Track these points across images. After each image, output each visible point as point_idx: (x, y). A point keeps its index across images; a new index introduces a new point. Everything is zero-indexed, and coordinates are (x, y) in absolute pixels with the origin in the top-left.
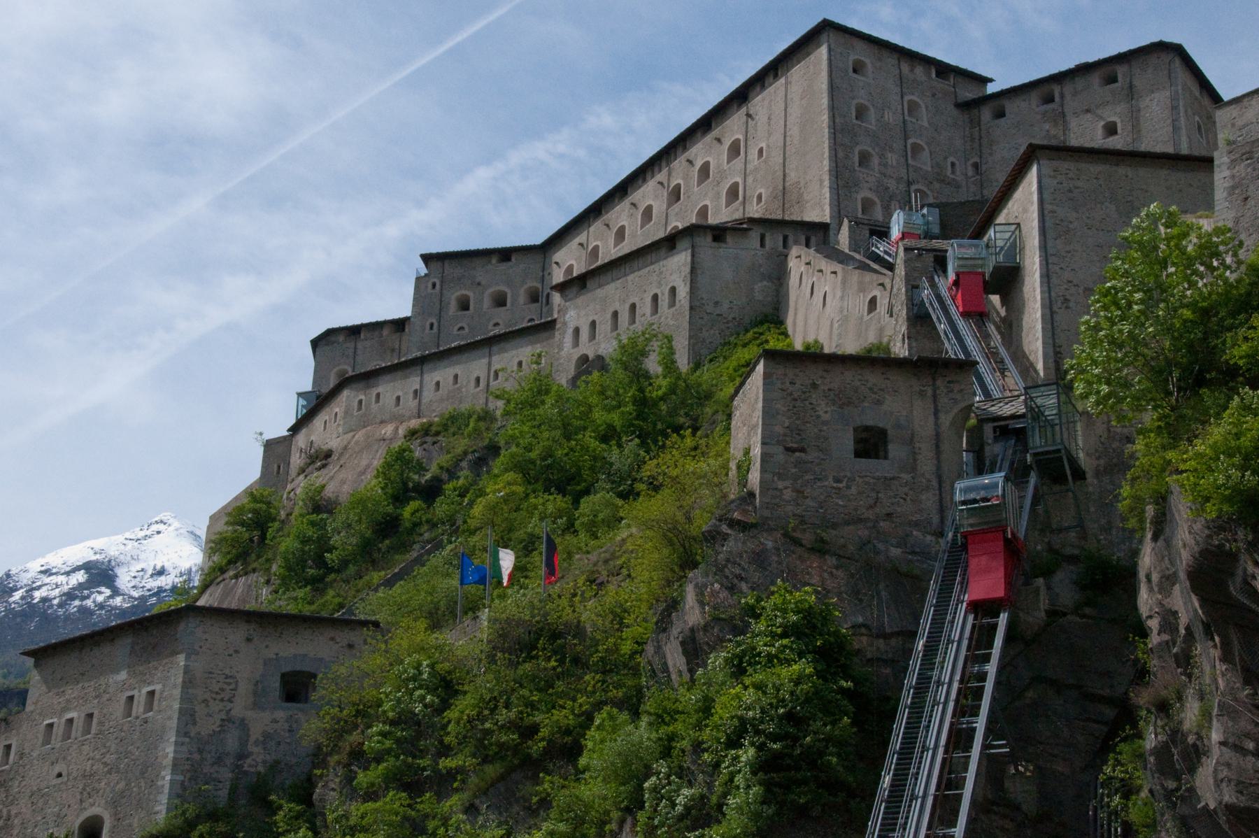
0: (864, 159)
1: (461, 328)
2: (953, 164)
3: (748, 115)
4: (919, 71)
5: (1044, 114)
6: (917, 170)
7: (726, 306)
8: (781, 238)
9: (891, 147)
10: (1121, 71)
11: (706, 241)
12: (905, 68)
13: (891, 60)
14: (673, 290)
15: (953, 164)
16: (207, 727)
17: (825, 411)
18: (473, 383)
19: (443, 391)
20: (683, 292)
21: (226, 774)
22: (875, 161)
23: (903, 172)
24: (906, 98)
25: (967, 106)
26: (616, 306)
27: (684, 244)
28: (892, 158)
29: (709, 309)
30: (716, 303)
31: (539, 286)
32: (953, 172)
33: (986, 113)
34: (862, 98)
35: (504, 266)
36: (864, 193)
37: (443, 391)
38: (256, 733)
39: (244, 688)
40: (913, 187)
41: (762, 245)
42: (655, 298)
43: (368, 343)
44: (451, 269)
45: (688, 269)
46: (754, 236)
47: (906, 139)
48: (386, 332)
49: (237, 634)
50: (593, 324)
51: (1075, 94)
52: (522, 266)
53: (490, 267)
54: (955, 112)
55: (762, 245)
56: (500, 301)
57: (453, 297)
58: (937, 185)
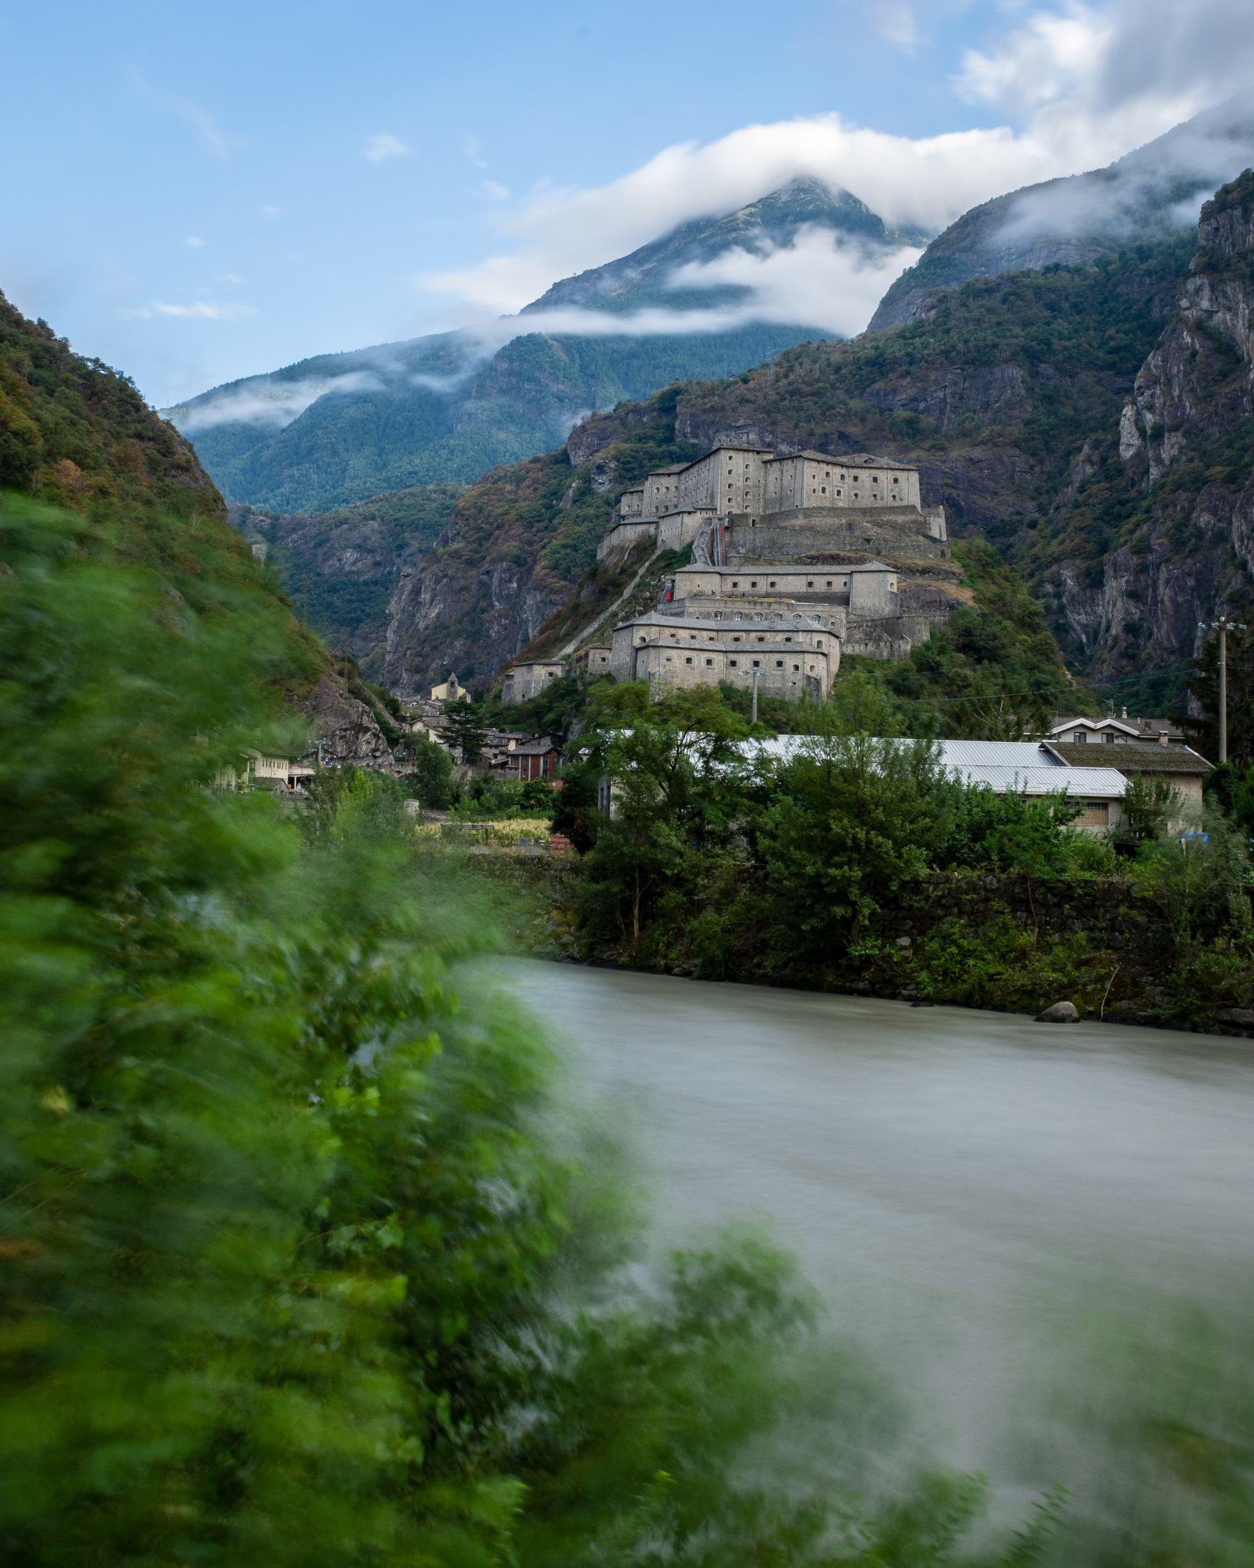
11: (686, 516)
13: (741, 454)
25: (765, 462)
28: (740, 484)
33: (769, 465)
44: (655, 479)
46: (699, 512)
56: (667, 488)
57: (655, 487)
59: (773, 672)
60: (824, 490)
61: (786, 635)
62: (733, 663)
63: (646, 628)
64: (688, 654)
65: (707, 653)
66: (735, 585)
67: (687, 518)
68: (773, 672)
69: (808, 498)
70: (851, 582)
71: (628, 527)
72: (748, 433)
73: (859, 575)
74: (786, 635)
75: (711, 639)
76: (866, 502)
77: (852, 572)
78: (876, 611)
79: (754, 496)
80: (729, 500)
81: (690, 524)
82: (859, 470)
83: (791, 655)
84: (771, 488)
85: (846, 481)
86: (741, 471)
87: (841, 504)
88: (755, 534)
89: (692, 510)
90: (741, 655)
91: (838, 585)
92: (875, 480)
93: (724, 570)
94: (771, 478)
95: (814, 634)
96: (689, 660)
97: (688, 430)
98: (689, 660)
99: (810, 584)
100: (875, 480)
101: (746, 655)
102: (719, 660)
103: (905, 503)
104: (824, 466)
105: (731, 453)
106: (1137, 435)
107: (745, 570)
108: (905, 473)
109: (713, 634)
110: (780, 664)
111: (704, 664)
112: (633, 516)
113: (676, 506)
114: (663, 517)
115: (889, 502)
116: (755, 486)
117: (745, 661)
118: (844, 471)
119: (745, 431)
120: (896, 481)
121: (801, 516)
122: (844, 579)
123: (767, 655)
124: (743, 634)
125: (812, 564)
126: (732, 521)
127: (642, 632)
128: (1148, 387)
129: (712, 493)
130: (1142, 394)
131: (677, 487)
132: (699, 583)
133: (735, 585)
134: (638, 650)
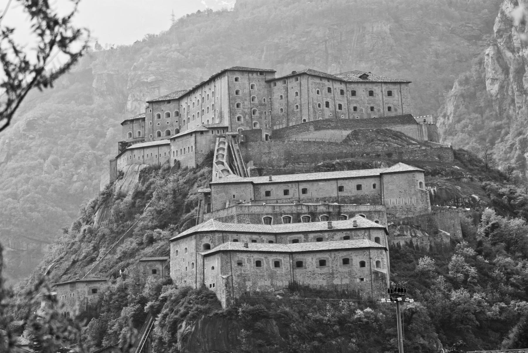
0: (238, 106)
1: (159, 124)
2: (264, 99)
3: (215, 86)
4: (255, 75)
5: (284, 87)
6: (253, 104)
7: (204, 151)
8: (217, 131)
9: (246, 100)
10: (299, 78)
11: (198, 135)
12: (250, 75)
13: (246, 75)
14: (192, 146)
15: (264, 99)
16: (82, 299)
17: (148, 268)
18: (155, 157)
19: (149, 158)
20: (194, 148)
21: (85, 306)
22: (241, 106)
23: (249, 106)
24: (250, 84)
25: (269, 82)
26: (181, 148)
27: (194, 135)
28: (246, 103)
29: (200, 153)
30: (201, 151)
31: (178, 111)
32: (264, 101)
33: (272, 84)
34: (237, 88)
35: (168, 105)
36: (238, 115)
37: (149, 158)
38: (89, 299)
39: (87, 293)
40: (252, 110)
41: (213, 133)
42: (189, 147)
43: (136, 124)
44: (155, 106)
45: (194, 142)
47: (250, 96)
48: (140, 121)
49: (84, 285)
50: (177, 151)
51: (290, 82)
52: (174, 105)
53: (165, 105)
54: (265, 84)
55: (213, 133)
56: (168, 115)
57: (156, 114)
58: (259, 107)
59: (340, 269)
60: (327, 105)
61: (344, 234)
62: (300, 264)
63: (210, 235)
64: (257, 257)
65: (274, 255)
66: (268, 194)
67: (199, 137)
68: (340, 269)
69: (315, 112)
70: (381, 184)
71: (136, 152)
72: (159, 88)
73: (389, 176)
74: (344, 234)
75: (271, 242)
76: (364, 112)
77: (382, 174)
78: (409, 210)
79: (261, 113)
80: (239, 119)
81: (204, 143)
82: (356, 85)
83: (357, 252)
84: (278, 105)
85: (345, 95)
86: (246, 91)
87: (343, 117)
88: (270, 148)
89: (204, 129)
90: (306, 255)
91: (368, 188)
92: (371, 93)
93: (257, 180)
94: (276, 95)
95: (371, 231)
96: (258, 264)
97: (104, 88)
98: (258, 264)
99: (341, 189)
100: (371, 93)
101: (312, 255)
102: (286, 262)
103: (399, 112)
104: (326, 82)
105: (238, 75)
106: (500, 70)
107: (276, 179)
108: (398, 86)
109: (272, 238)
110: (346, 261)
111: (272, 265)
112: (136, 142)
113: (178, 131)
114: (174, 139)
115: (387, 114)
116: (261, 105)
117: (311, 262)
118: (343, 87)
119: (156, 86)
120: (390, 94)
121: (312, 128)
122: (372, 181)
123: (333, 253)
124: (302, 236)
125: (328, 171)
126: (246, 137)
127: (206, 240)
128: (506, 30)
129: (221, 113)
130: (501, 36)
131: (177, 114)
132: (234, 193)
133: (268, 194)
134: (205, 256)
